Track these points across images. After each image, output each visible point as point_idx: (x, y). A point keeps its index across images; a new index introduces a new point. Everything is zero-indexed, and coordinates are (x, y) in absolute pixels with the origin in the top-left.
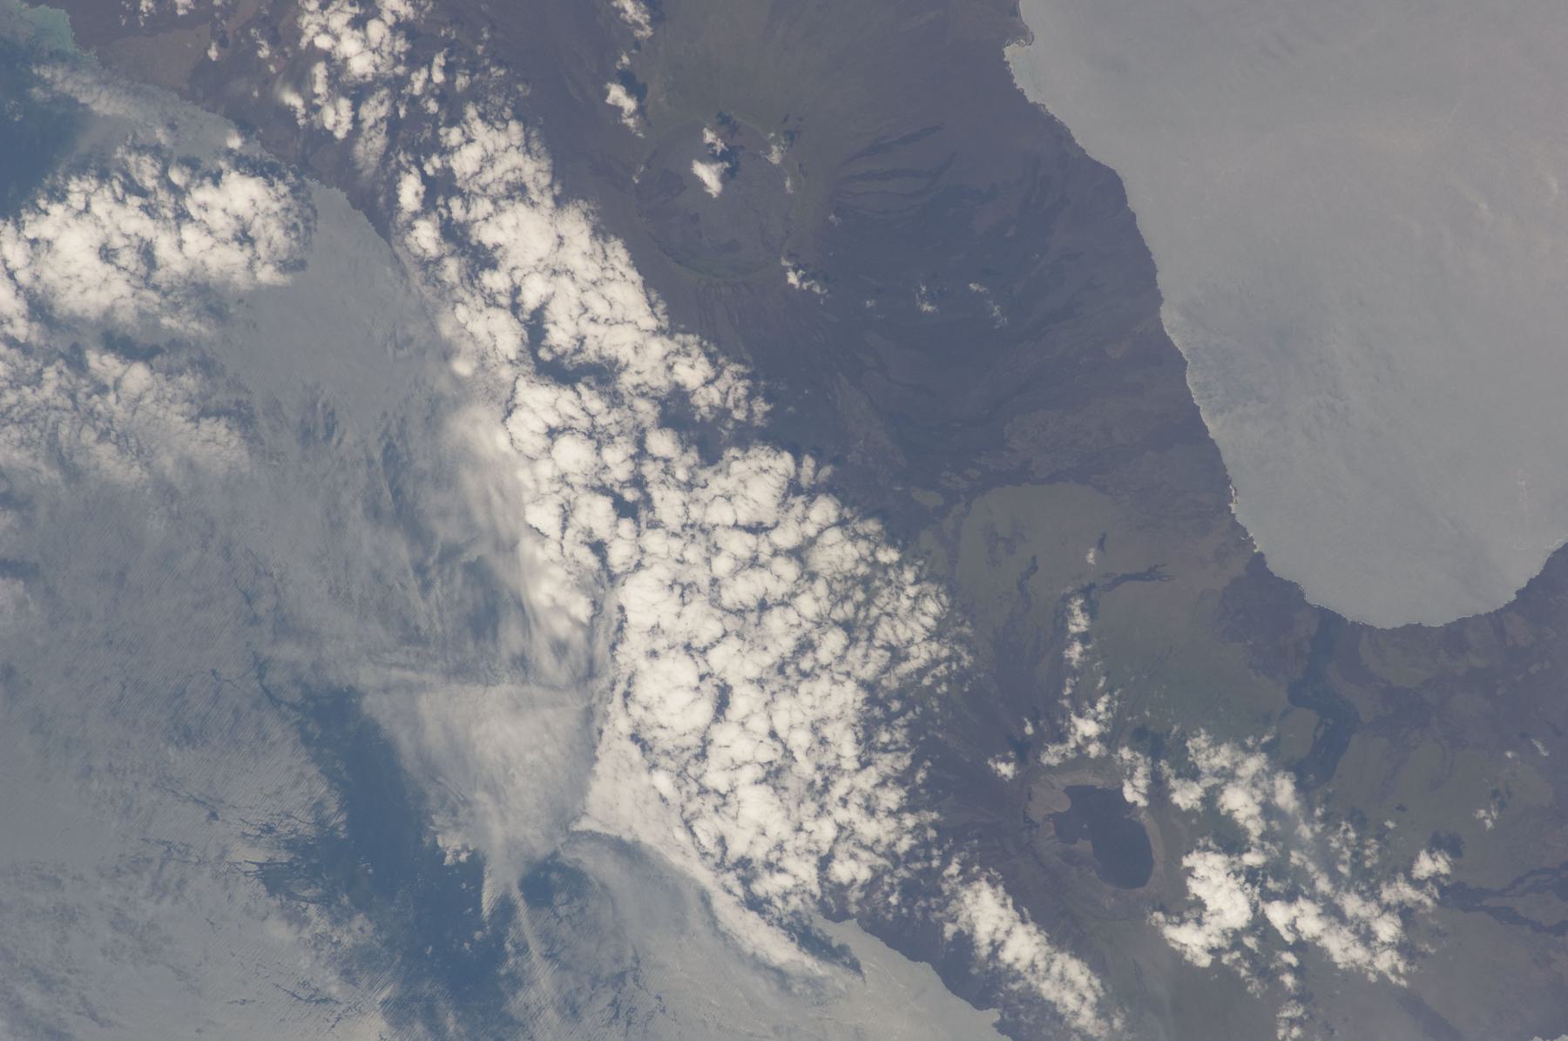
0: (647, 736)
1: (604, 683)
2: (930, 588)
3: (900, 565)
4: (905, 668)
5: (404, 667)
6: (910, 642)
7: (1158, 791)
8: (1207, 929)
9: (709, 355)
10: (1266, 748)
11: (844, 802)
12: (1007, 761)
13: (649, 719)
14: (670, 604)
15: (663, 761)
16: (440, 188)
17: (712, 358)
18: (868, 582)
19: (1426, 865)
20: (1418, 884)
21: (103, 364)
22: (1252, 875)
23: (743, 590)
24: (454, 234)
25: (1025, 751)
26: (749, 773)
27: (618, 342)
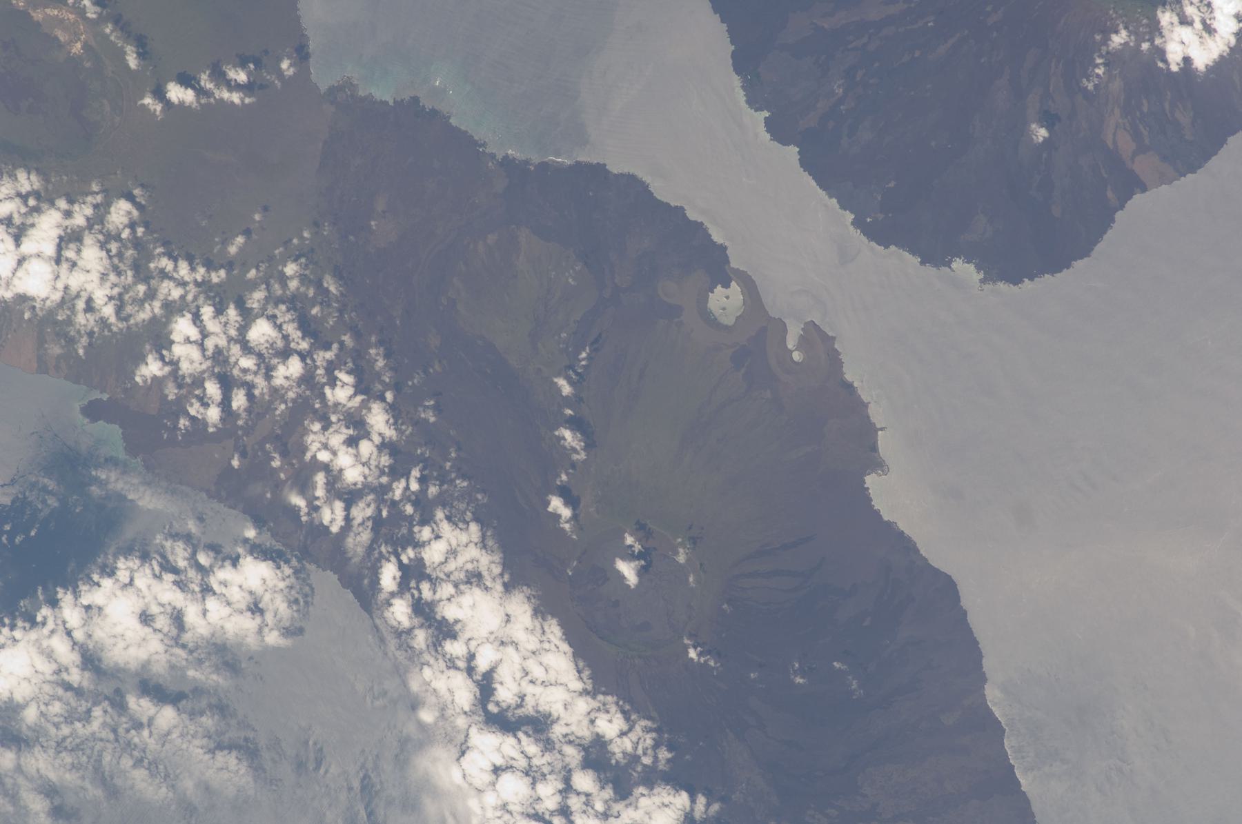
9: (623, 712)
16: (413, 574)
17: (626, 715)
21: (140, 706)
24: (423, 610)
27: (551, 700)
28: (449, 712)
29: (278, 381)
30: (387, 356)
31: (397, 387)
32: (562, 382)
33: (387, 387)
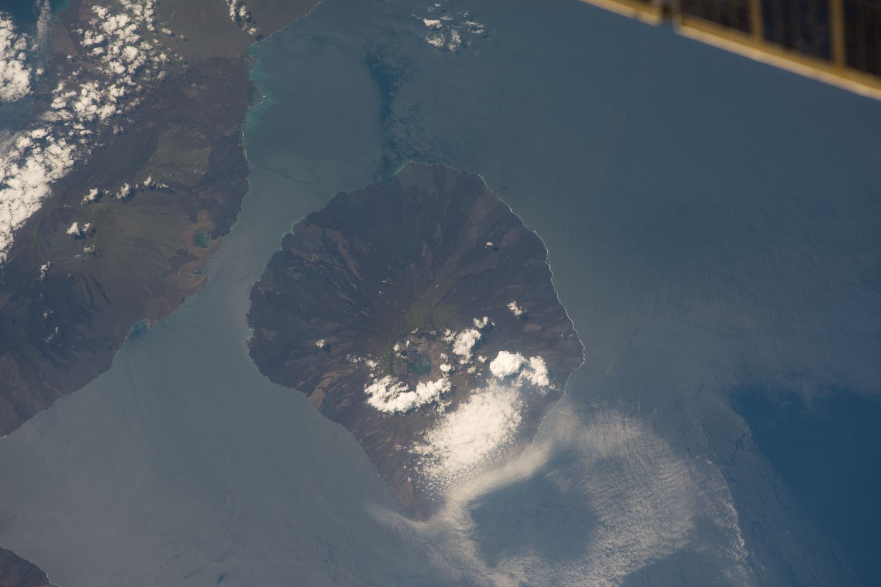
29: (112, 64)
30: (137, 107)
31: (123, 115)
33: (123, 110)
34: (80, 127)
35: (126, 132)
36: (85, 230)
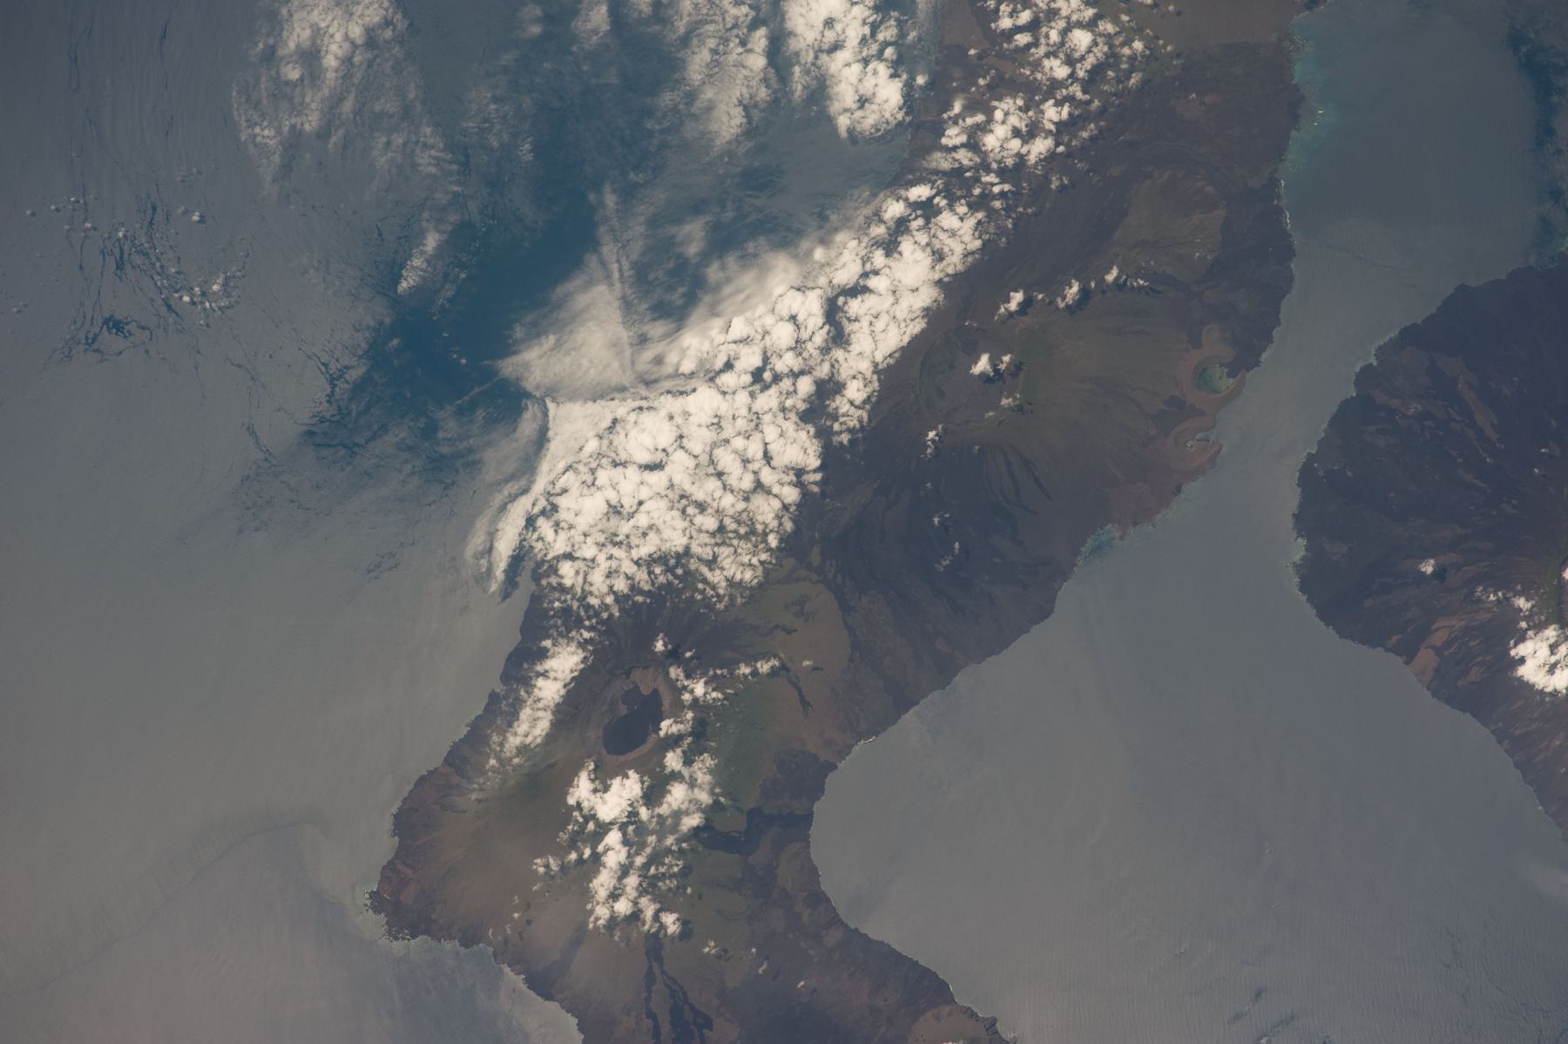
0: (618, 428)
1: (643, 392)
2: (760, 572)
3: (769, 549)
4: (705, 570)
5: (620, 270)
6: (722, 569)
7: (673, 741)
8: (592, 797)
9: (869, 398)
10: (716, 802)
11: (610, 558)
12: (665, 645)
13: (629, 426)
14: (706, 418)
15: (605, 442)
16: (927, 210)
17: (867, 400)
18: (753, 533)
19: (669, 919)
20: (656, 918)
22: (633, 814)
23: (726, 460)
24: (901, 226)
25: (673, 656)
26: (613, 496)
27: (861, 341)
28: (827, 269)
30: (1092, 139)
31: (1069, 154)
32: (1115, 272)
33: (1068, 145)
34: (992, 178)
35: (1073, 185)
36: (1002, 367)
